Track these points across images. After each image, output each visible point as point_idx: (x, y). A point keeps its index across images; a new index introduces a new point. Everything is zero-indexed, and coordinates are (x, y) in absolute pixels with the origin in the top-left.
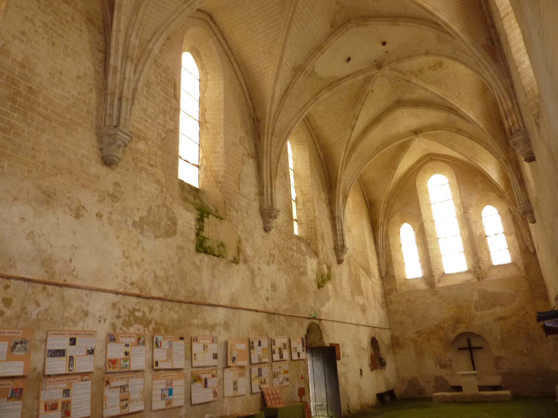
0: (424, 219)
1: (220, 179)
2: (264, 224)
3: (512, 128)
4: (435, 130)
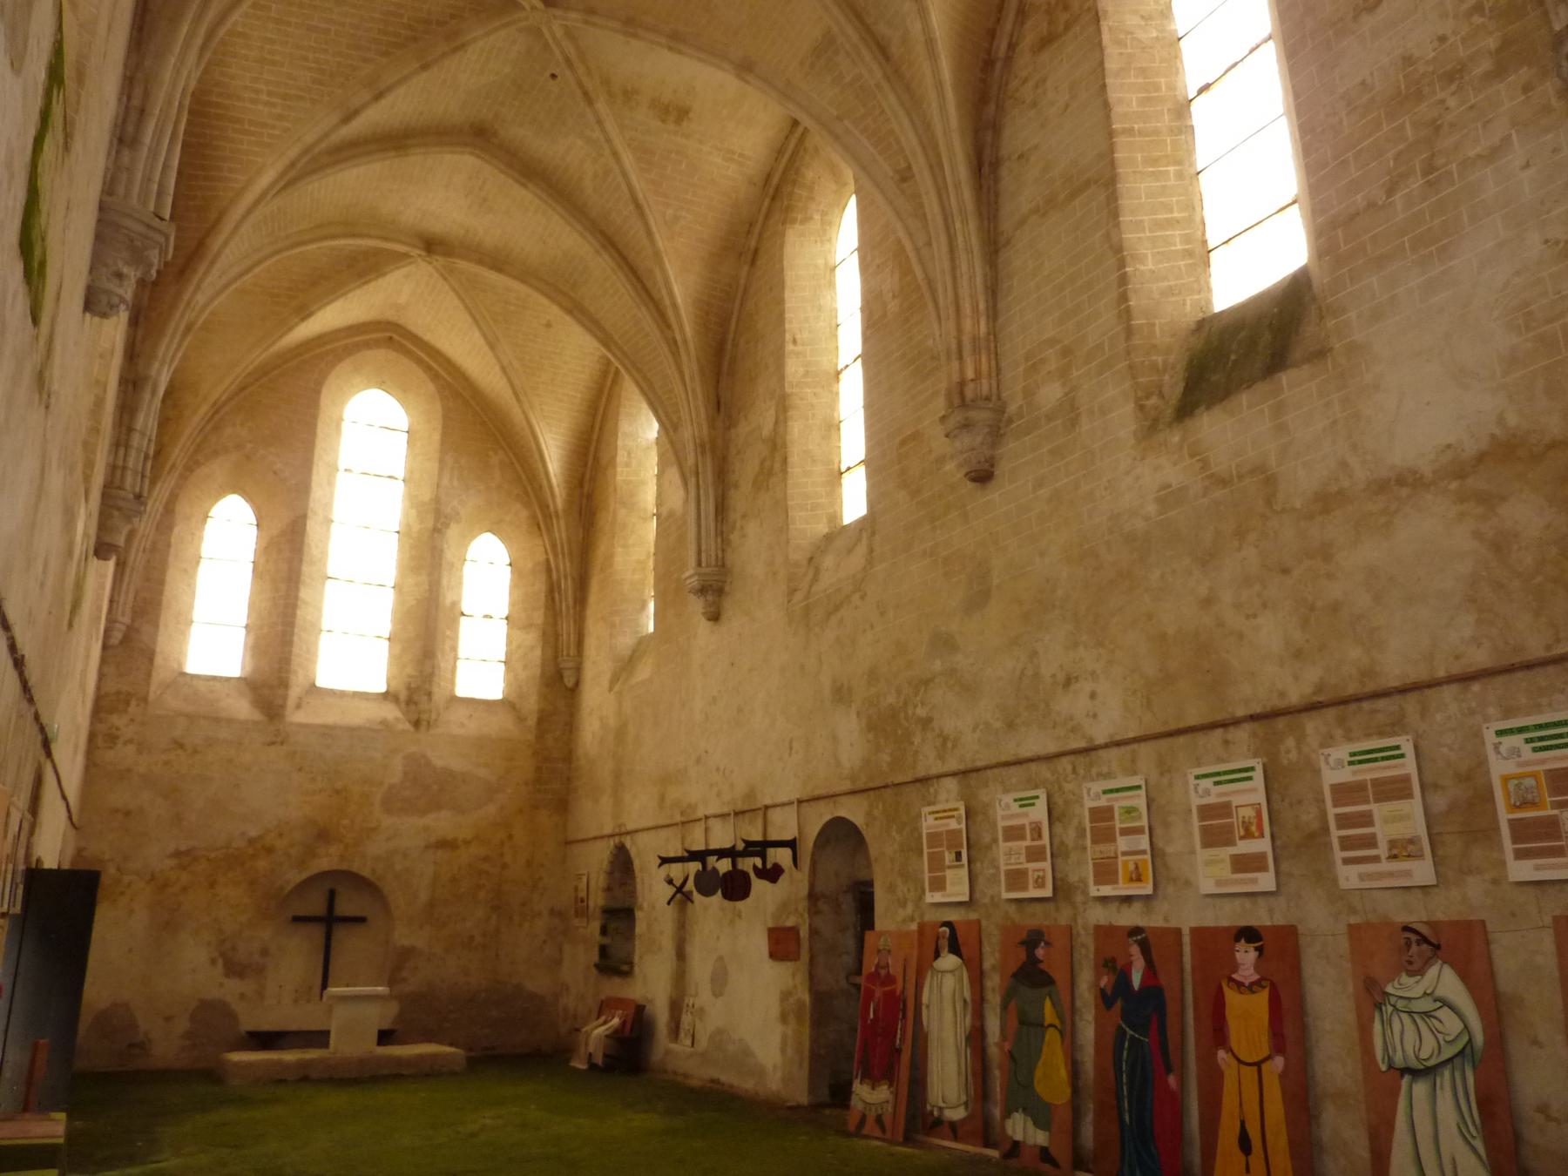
0: (311, 505)
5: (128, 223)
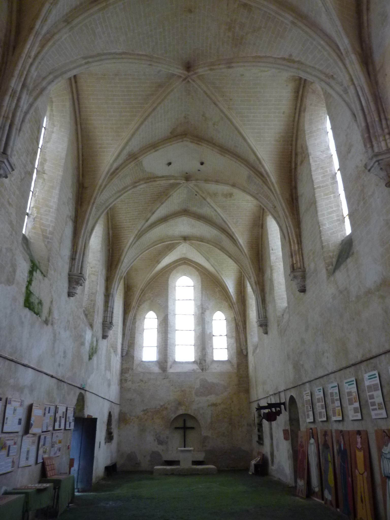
0: (169, 311)
2: (69, 288)
3: (295, 265)
5: (74, 277)
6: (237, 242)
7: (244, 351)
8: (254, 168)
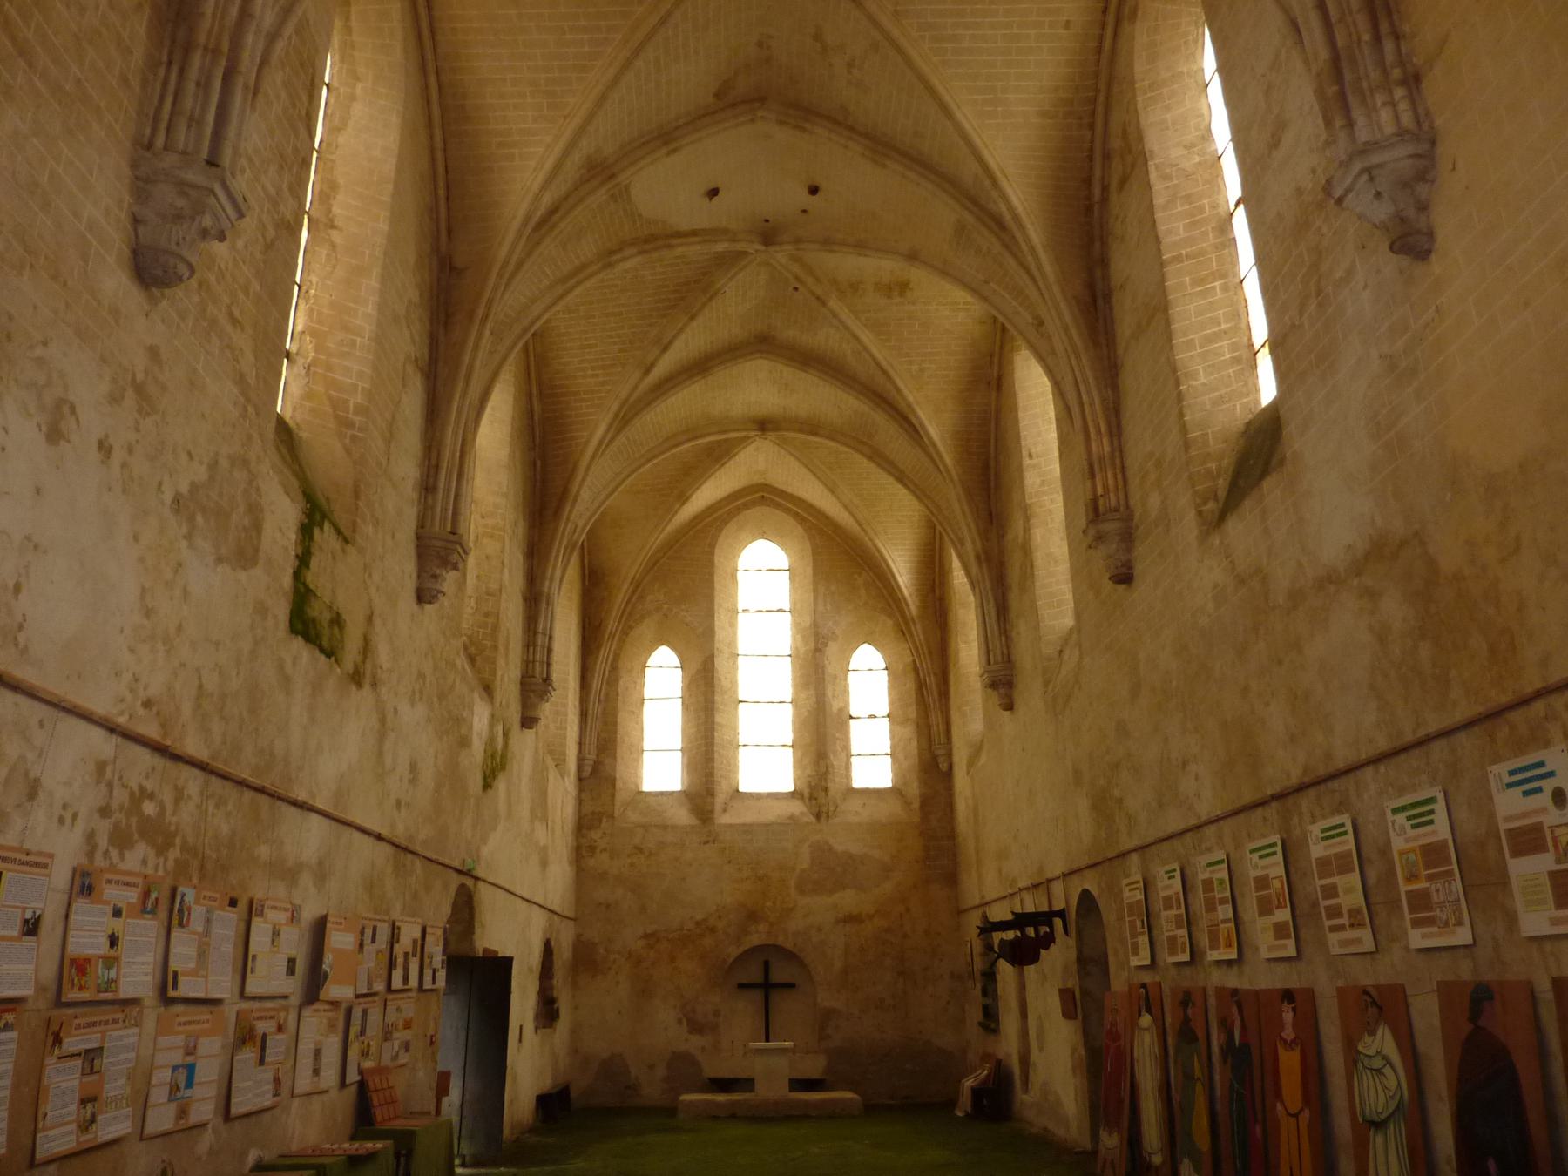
0: (717, 645)
1: (350, 416)
3: (1101, 502)
4: (815, 434)
6: (922, 433)
7: (941, 759)
8: (976, 203)
